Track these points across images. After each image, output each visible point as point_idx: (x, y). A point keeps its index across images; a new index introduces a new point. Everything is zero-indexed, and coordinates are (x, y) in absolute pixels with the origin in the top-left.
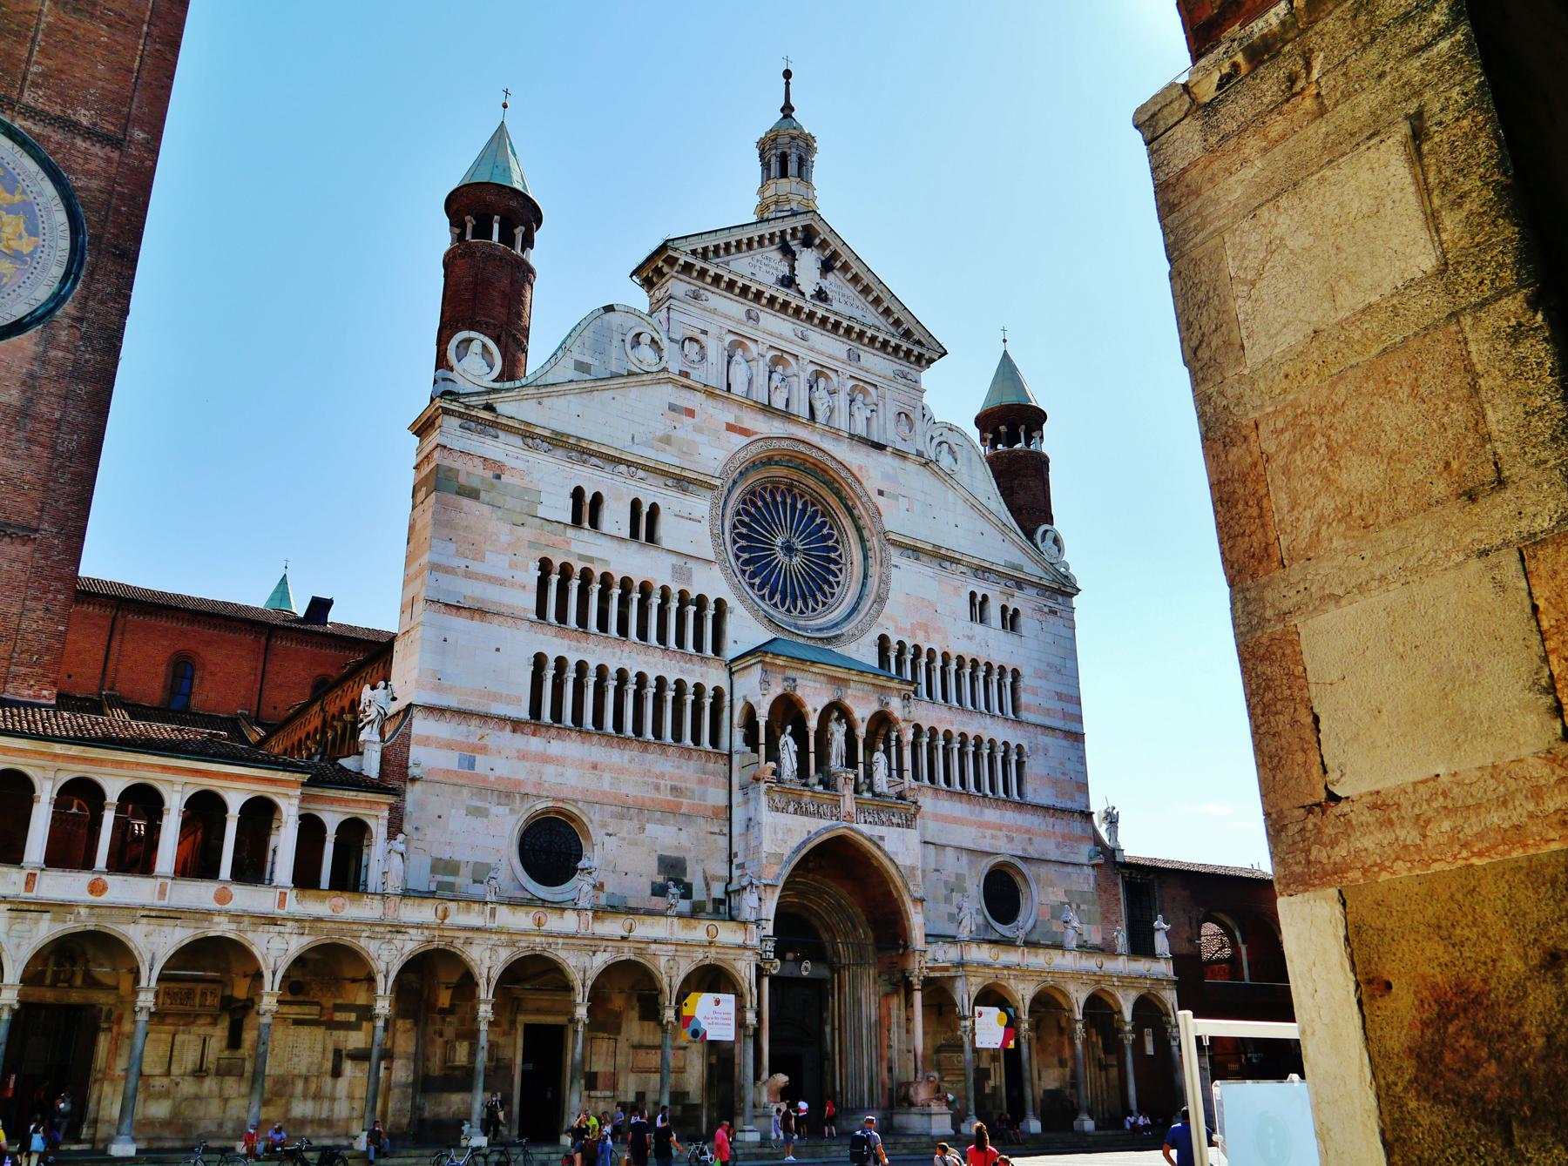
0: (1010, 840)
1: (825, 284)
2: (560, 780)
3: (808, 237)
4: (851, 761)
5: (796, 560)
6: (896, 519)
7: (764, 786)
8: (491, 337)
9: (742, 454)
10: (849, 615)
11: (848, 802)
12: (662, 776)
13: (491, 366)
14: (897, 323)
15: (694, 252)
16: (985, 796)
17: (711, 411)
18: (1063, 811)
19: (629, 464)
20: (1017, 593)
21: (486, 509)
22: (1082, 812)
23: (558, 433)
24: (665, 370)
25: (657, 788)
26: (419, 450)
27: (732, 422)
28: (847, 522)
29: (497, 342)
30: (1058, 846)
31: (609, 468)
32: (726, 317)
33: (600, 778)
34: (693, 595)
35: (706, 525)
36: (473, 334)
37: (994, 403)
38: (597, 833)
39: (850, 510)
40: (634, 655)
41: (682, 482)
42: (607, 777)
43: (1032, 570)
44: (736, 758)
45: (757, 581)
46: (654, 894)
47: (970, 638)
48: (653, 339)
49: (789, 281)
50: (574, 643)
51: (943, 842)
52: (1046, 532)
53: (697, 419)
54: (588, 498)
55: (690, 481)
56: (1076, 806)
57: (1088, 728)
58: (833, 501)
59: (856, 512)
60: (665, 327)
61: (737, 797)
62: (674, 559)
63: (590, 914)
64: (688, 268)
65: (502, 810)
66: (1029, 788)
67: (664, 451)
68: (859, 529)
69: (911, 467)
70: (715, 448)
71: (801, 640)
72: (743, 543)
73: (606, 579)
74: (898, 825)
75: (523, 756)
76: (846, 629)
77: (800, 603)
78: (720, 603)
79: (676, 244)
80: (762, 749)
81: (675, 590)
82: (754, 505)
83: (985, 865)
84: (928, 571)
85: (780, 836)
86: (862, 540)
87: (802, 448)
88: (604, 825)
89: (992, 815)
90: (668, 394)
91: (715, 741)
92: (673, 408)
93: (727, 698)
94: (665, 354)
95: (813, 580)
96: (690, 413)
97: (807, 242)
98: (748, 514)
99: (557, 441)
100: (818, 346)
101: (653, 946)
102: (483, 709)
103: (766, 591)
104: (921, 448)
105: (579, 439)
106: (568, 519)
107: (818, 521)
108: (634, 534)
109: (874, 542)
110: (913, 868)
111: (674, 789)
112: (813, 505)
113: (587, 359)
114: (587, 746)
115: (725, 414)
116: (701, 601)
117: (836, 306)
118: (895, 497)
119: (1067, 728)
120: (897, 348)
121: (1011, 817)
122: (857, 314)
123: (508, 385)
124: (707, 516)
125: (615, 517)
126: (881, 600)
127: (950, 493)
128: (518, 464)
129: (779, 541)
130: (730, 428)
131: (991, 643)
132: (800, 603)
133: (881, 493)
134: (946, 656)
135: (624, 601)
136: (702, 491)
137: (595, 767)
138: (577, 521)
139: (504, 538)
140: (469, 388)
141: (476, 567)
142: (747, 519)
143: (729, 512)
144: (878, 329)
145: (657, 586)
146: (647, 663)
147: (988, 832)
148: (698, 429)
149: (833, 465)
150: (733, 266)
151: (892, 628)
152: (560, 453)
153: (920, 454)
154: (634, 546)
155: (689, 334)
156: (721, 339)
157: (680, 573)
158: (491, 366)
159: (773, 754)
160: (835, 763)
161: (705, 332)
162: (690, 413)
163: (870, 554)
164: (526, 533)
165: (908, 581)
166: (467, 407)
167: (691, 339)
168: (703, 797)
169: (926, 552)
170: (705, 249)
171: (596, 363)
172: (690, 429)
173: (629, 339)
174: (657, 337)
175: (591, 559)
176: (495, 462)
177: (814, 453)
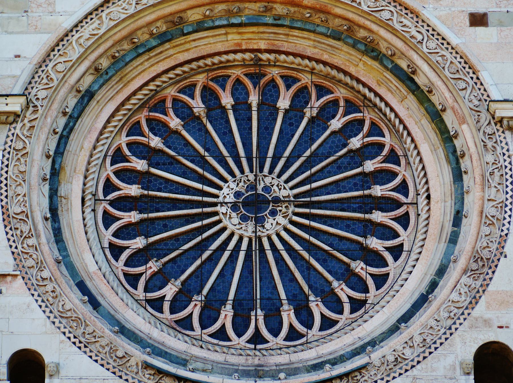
5: (274, 225)
10: (406, 318)
28: (407, 109)
39: (407, 78)
45: (170, 291)
58: (366, 70)
59: (420, 80)
68: (436, 116)
76: (375, 356)
82: (158, 127)
86: (447, 137)
95: (325, 258)
103: (194, 309)
107: (336, 124)
109: (467, 138)
112: (322, 91)
126: (484, 265)
129: (227, 193)
133: (478, 20)
163: (465, 164)
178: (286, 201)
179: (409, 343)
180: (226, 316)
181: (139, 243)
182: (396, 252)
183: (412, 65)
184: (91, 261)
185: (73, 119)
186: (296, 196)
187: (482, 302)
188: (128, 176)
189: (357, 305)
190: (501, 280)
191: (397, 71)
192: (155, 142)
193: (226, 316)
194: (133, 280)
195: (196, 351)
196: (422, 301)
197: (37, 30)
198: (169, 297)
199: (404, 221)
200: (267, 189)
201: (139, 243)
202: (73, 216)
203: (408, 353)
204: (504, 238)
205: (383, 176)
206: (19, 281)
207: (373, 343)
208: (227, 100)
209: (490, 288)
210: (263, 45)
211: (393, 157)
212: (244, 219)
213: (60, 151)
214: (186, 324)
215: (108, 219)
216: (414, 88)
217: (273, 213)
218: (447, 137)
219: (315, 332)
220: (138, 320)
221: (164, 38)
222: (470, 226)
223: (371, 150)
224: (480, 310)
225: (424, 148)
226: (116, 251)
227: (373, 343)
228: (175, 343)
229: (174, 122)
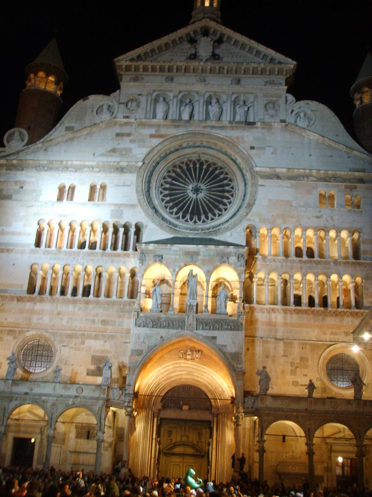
1: (217, 51)
2: (40, 322)
5: (201, 196)
9: (159, 148)
10: (231, 218)
12: (97, 315)
13: (23, 140)
15: (132, 60)
25: (93, 322)
28: (235, 168)
29: (28, 129)
33: (62, 319)
38: (58, 346)
42: (66, 318)
45: (175, 210)
46: (88, 374)
47: (318, 217)
48: (109, 106)
53: (132, 137)
59: (238, 162)
60: (117, 99)
63: (10, 382)
64: (128, 69)
65: (10, 338)
67: (111, 156)
68: (241, 170)
75: (21, 312)
77: (203, 217)
85: (142, 340)
86: (243, 176)
88: (61, 342)
92: (118, 135)
96: (129, 135)
101: (44, 398)
103: (181, 214)
109: (248, 176)
111: (104, 322)
125: (82, 192)
126: (250, 206)
129: (190, 187)
130: (152, 136)
133: (252, 148)
137: (59, 314)
138: (60, 199)
147: (328, 331)
148: (132, 141)
155: (131, 97)
161: (140, 95)
168: (121, 324)
173: (95, 110)
174: (111, 104)
178: (204, 189)
179: (231, 224)
180: (188, 216)
181: (168, 198)
182: (230, 203)
183: (236, 159)
184: (156, 202)
185: (155, 168)
186: (207, 189)
187: (249, 214)
188: (167, 183)
189: (219, 215)
190: (254, 210)
191: (232, 159)
193: (188, 216)
194: (166, 207)
195: (180, 224)
196: (235, 214)
198: (175, 211)
199: (232, 195)
200: (200, 187)
201: (168, 198)
202: (153, 192)
203: (230, 226)
204: (255, 200)
205: (228, 185)
206: (139, 206)
207: (223, 224)
208: (191, 166)
209: (251, 211)
211: (231, 180)
212: (194, 193)
213: (150, 176)
214: (178, 218)
215: (161, 193)
216: (236, 163)
217: (201, 192)
218: (243, 176)
219: (209, 221)
220: (167, 216)
221: (177, 150)
222: (248, 197)
223: (225, 179)
224: (248, 216)
225: (238, 178)
226: (163, 200)
227: (223, 224)
228: (176, 222)
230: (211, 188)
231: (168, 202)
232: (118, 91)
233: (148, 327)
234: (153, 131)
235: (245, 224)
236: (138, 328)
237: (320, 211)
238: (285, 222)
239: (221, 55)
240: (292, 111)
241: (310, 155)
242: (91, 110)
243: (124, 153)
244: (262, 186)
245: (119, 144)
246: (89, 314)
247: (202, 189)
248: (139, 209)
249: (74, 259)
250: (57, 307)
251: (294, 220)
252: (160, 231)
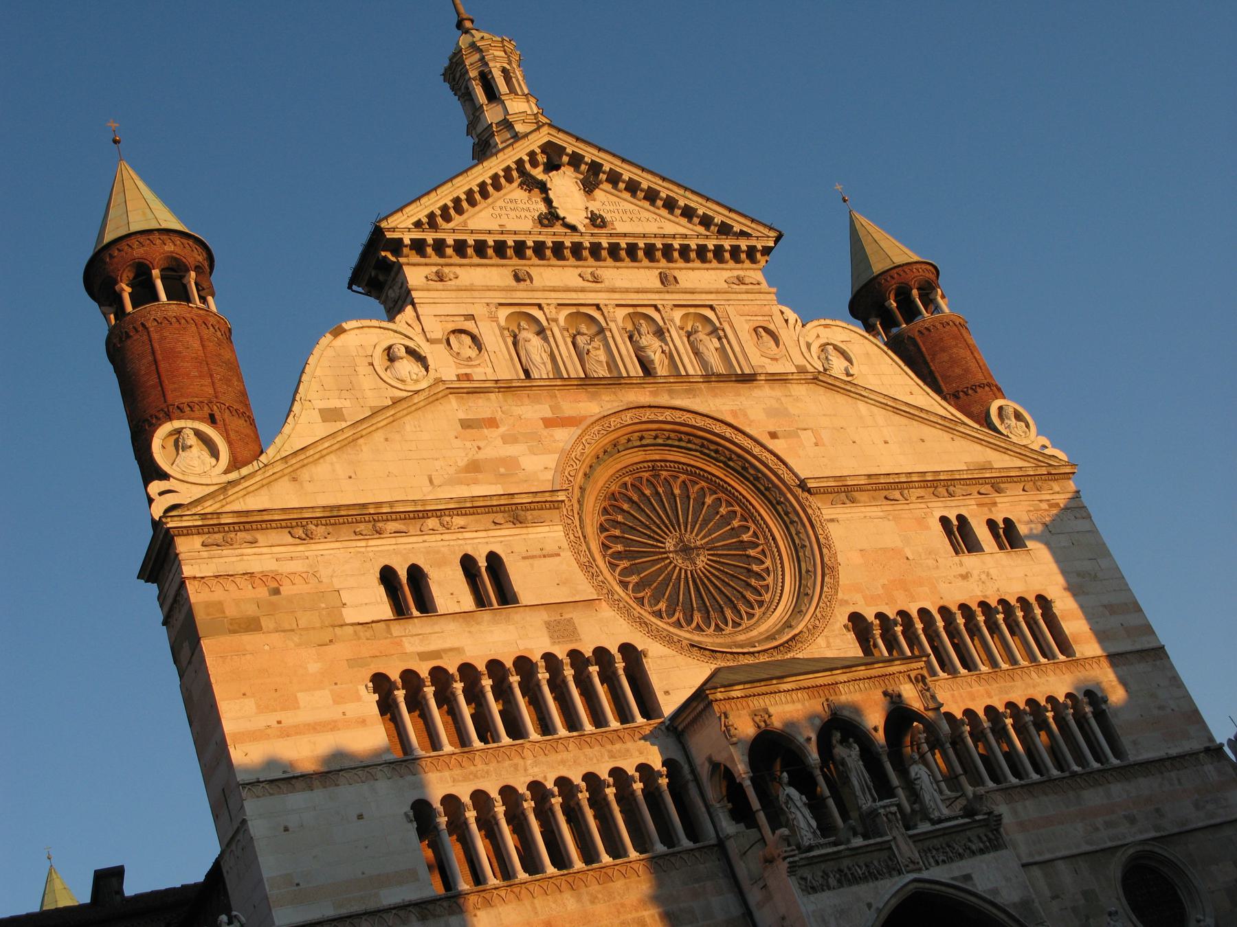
0: (1132, 820)
1: (594, 206)
3: (553, 158)
4: (883, 788)
5: (701, 561)
6: (806, 460)
7: (784, 866)
8: (201, 420)
11: (906, 850)
13: (215, 453)
14: (706, 221)
15: (418, 224)
16: (1074, 774)
17: (517, 410)
18: (1181, 757)
19: (438, 513)
20: (999, 499)
21: (275, 638)
22: (1207, 750)
23: (332, 508)
24: (439, 381)
26: (161, 599)
27: (549, 414)
30: (1197, 806)
31: (413, 527)
32: (489, 289)
34: (588, 653)
35: (567, 555)
36: (177, 424)
37: (856, 289)
40: (542, 758)
41: (513, 511)
43: (1002, 461)
44: (732, 846)
47: (965, 577)
48: (410, 352)
49: (551, 217)
50: (457, 772)
51: (1048, 856)
52: (1000, 408)
53: (502, 429)
54: (403, 575)
55: (528, 507)
56: (1195, 745)
57: (1166, 636)
60: (418, 329)
61: (754, 896)
62: (544, 615)
66: (1126, 741)
67: (476, 482)
69: (799, 390)
70: (539, 449)
71: (750, 660)
72: (624, 564)
73: (467, 671)
74: (982, 852)
77: (729, 613)
78: (627, 650)
79: (392, 222)
80: (762, 817)
81: (561, 653)
83: (1115, 870)
84: (875, 511)
87: (649, 415)
89: (1093, 797)
90: (455, 409)
91: (693, 832)
92: (466, 424)
93: (686, 768)
94: (430, 361)
96: (492, 423)
97: (552, 166)
98: (616, 524)
99: (338, 519)
100: (619, 284)
102: (372, 905)
104: (800, 361)
105: (364, 506)
106: (386, 611)
108: (481, 601)
110: (1026, 904)
113: (334, 403)
114: (527, 903)
115: (532, 411)
116: (601, 654)
117: (621, 228)
118: (792, 435)
119: (1138, 647)
120: (718, 252)
121: (1119, 790)
122: (651, 228)
123: (245, 471)
124: (565, 545)
125: (450, 590)
127: (862, 407)
128: (297, 566)
129: (670, 544)
130: (549, 423)
131: (993, 572)
132: (729, 613)
133: (773, 435)
134: (944, 610)
135: (502, 691)
136: (546, 514)
138: (400, 611)
139: (314, 667)
140: (198, 492)
141: (289, 718)
142: (617, 532)
143: (591, 530)
144: (685, 236)
145: (536, 657)
146: (563, 762)
148: (509, 439)
149: (700, 422)
150: (472, 225)
151: (861, 602)
152: (346, 531)
153: (802, 370)
154: (486, 615)
156: (494, 319)
157: (560, 629)
158: (215, 453)
159: (777, 818)
160: (866, 803)
161: (471, 317)
162: (492, 423)
164: (341, 651)
165: (850, 533)
166: (204, 516)
167: (454, 332)
169: (859, 488)
170: (431, 216)
171: (347, 403)
172: (499, 442)
174: (411, 344)
175: (437, 654)
176: (264, 575)
177: (668, 415)
186: (707, 543)
192: (620, 518)
197: (550, 452)
210: (657, 457)
217: (698, 555)
224: (840, 595)
229: (626, 507)
230: (712, 541)
231: (639, 587)
232: (409, 308)
233: (829, 889)
234: (544, 410)
235: (842, 618)
236: (813, 897)
237: (961, 564)
238: (913, 599)
239: (608, 217)
240: (809, 346)
241: (886, 442)
242: (366, 361)
243: (502, 470)
244: (832, 520)
245: (479, 448)
246: (623, 905)
247: (697, 548)
248: (606, 611)
249: (516, 767)
250: (534, 908)
251: (926, 589)
252: (681, 660)
